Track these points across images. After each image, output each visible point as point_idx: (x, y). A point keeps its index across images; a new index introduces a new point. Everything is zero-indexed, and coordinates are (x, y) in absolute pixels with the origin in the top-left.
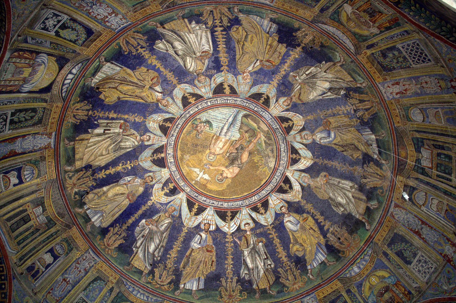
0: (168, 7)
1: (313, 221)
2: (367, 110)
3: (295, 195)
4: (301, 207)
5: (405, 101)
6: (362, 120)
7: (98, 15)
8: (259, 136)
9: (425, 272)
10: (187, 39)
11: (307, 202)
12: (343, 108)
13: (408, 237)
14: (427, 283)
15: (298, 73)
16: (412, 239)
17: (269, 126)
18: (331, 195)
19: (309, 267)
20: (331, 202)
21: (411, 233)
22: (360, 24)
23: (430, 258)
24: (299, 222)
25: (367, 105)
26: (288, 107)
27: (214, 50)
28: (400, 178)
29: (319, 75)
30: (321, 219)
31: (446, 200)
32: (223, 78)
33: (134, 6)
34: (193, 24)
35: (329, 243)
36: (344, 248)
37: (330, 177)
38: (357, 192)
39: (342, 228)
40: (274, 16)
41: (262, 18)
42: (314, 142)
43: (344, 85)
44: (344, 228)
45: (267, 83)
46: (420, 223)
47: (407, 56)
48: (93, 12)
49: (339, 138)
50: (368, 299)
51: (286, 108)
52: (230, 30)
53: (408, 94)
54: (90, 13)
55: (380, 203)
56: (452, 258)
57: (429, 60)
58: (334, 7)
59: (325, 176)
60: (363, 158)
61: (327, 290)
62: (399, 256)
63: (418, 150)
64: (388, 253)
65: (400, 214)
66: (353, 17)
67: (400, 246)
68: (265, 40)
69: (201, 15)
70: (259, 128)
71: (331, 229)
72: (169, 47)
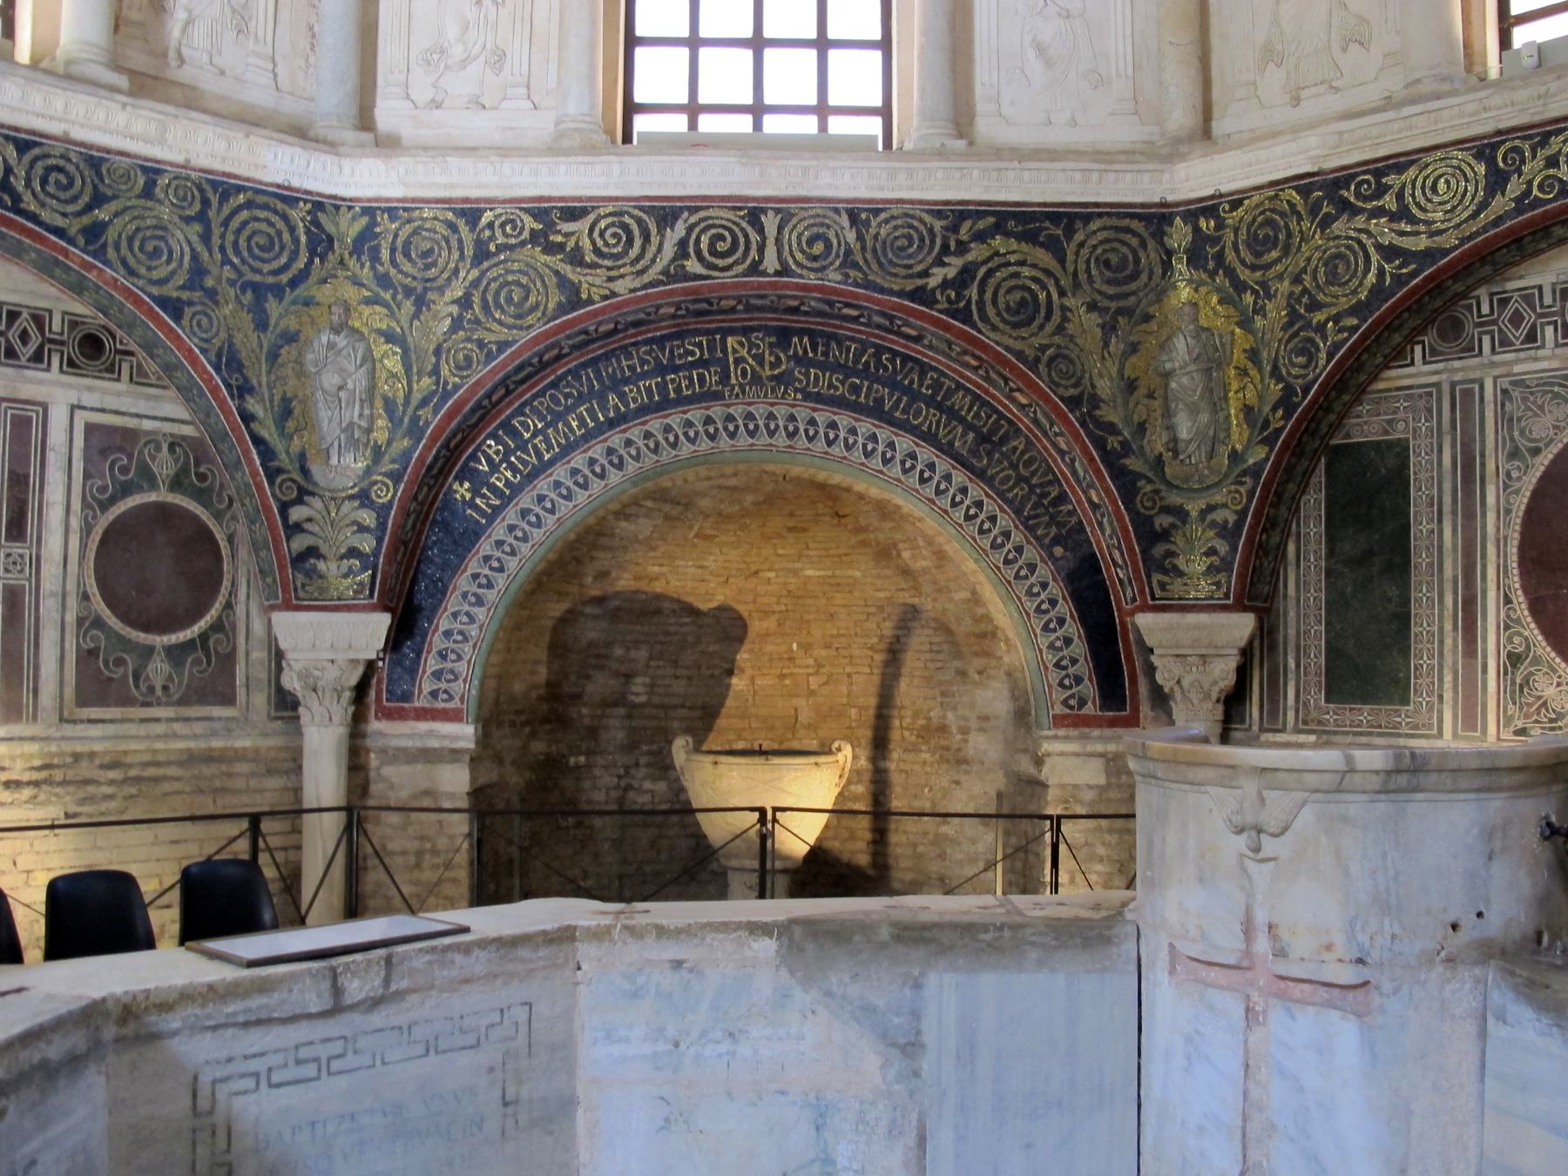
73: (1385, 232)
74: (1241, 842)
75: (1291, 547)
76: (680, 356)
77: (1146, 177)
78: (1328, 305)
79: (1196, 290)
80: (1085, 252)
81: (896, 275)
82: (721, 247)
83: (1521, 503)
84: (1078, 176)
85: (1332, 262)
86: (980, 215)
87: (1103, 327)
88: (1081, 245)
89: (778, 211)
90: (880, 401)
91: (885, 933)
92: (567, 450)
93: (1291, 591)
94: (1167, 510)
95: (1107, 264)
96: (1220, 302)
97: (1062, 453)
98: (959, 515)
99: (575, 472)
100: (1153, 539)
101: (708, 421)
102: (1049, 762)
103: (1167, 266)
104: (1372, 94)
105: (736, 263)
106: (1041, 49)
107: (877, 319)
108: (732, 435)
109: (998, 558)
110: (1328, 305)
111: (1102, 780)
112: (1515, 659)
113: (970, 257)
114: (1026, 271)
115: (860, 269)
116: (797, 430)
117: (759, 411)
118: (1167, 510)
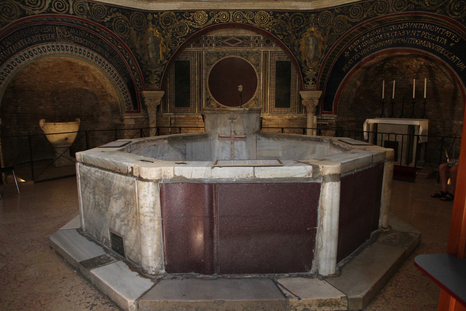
74: (230, 121)
75: (168, 79)
76: (45, 30)
82: (60, 6)
83: (209, 73)
86: (114, 7)
87: (137, 34)
88: (133, 16)
90: (90, 45)
91: (181, 138)
92: (18, 51)
93: (168, 87)
94: (148, 71)
95: (137, 21)
97: (126, 58)
98: (106, 70)
99: (21, 56)
100: (146, 76)
101: (53, 46)
102: (125, 120)
103: (148, 23)
105: (63, 11)
107: (91, 27)
108: (58, 50)
109: (114, 80)
111: (134, 123)
112: (208, 99)
113: (112, 16)
116: (73, 50)
117: (64, 45)
118: (148, 71)
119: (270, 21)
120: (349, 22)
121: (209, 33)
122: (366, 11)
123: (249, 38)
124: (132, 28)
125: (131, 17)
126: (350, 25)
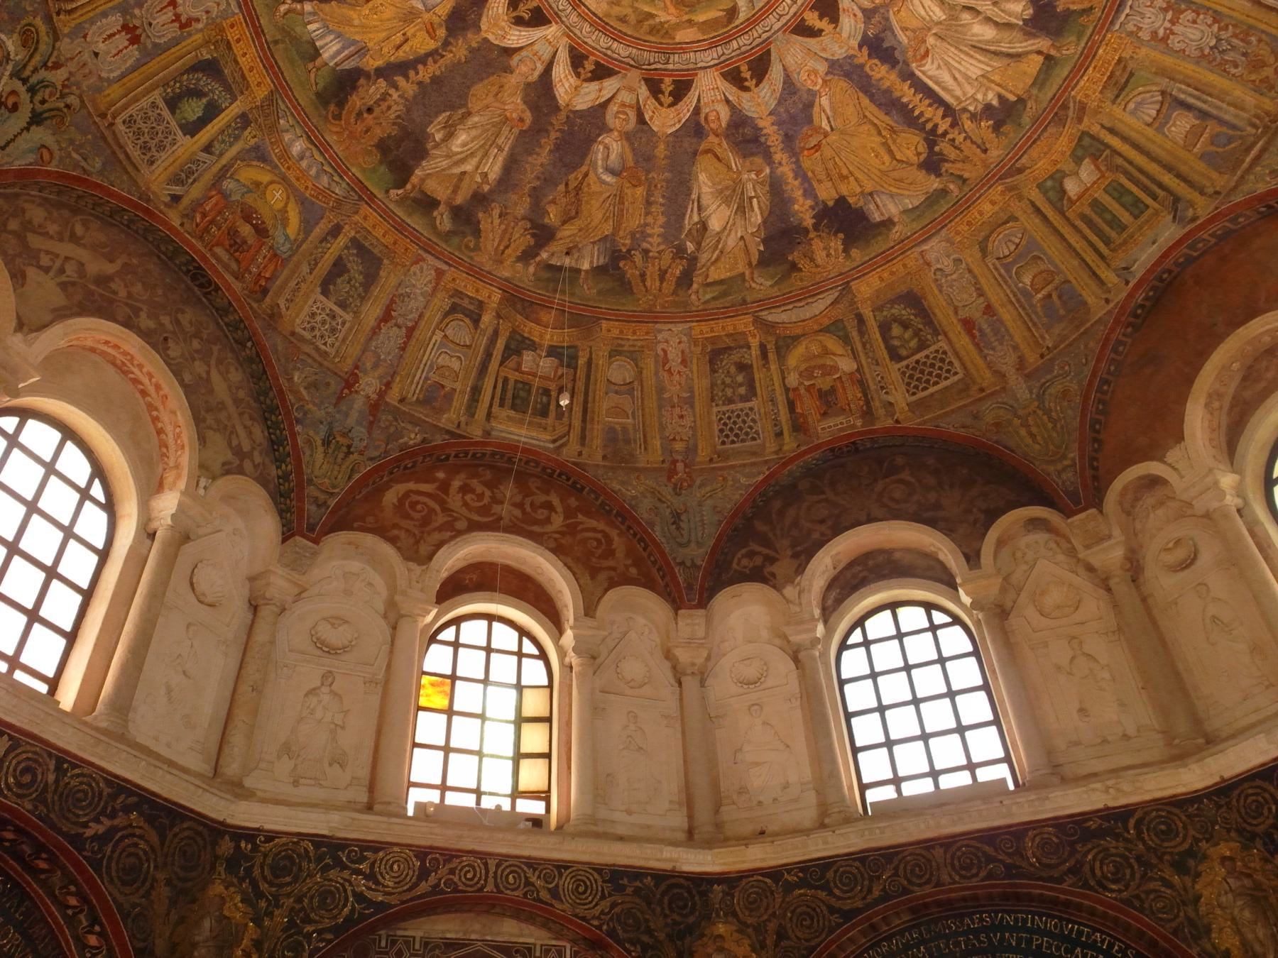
0: (1065, 107)
1: (423, 52)
2: (643, 275)
3: (496, 25)
4: (465, 29)
5: (649, 365)
6: (624, 258)
7: (1194, 22)
8: (672, 10)
9: (313, 329)
10: (977, 56)
11: (472, 50)
12: (658, 230)
13: (376, 291)
14: (293, 334)
15: (762, 183)
16: (375, 301)
17: (682, 48)
18: (476, 119)
19: (308, 7)
20: (460, 112)
21: (385, 300)
22: (813, 363)
23: (344, 340)
24: (428, 10)
25: (652, 283)
26: (703, 116)
27: (912, 76)
28: (497, 296)
29: (740, 222)
30: (424, 74)
31: (462, 388)
32: (845, 35)
33: (1131, 75)
34: (992, 98)
35: (362, 81)
36: (348, 123)
37: (516, 131)
38: (475, 186)
39: (394, 124)
40: (896, 233)
41: (906, 211)
42: (604, 129)
43: (704, 257)
44: (395, 131)
45: (775, 109)
46: (410, 324)
47: (732, 407)
48: (1210, 26)
49: (598, 189)
50: (231, 177)
51: (705, 110)
52: (926, 139)
53: (661, 372)
54: (1215, 21)
55: (447, 236)
56: (357, 392)
57: (723, 443)
58: (859, 347)
59: (521, 120)
60: (544, 228)
61: (247, 56)
62: (334, 265)
63: (553, 352)
64: (340, 238)
65: (421, 278)
66: (829, 362)
67: (355, 268)
68: (860, 176)
69: (997, 128)
70: (690, 21)
71: (395, 95)
72: (998, 16)
73: (361, 884)
77: (223, 803)
78: (316, 922)
79: (227, 888)
80: (176, 840)
81: (67, 819)
84: (192, 788)
85: (325, 895)
86: (131, 793)
88: (175, 835)
89: (11, 738)
96: (242, 901)
103: (213, 868)
104: (343, 796)
106: (169, 691)
110: (316, 922)
113: (116, 822)
114: (142, 845)
115: (46, 806)
119: (603, 897)
120: (832, 910)
121: (402, 925)
122: (879, 878)
123: (529, 950)
124: (161, 876)
125: (169, 837)
126: (835, 918)
